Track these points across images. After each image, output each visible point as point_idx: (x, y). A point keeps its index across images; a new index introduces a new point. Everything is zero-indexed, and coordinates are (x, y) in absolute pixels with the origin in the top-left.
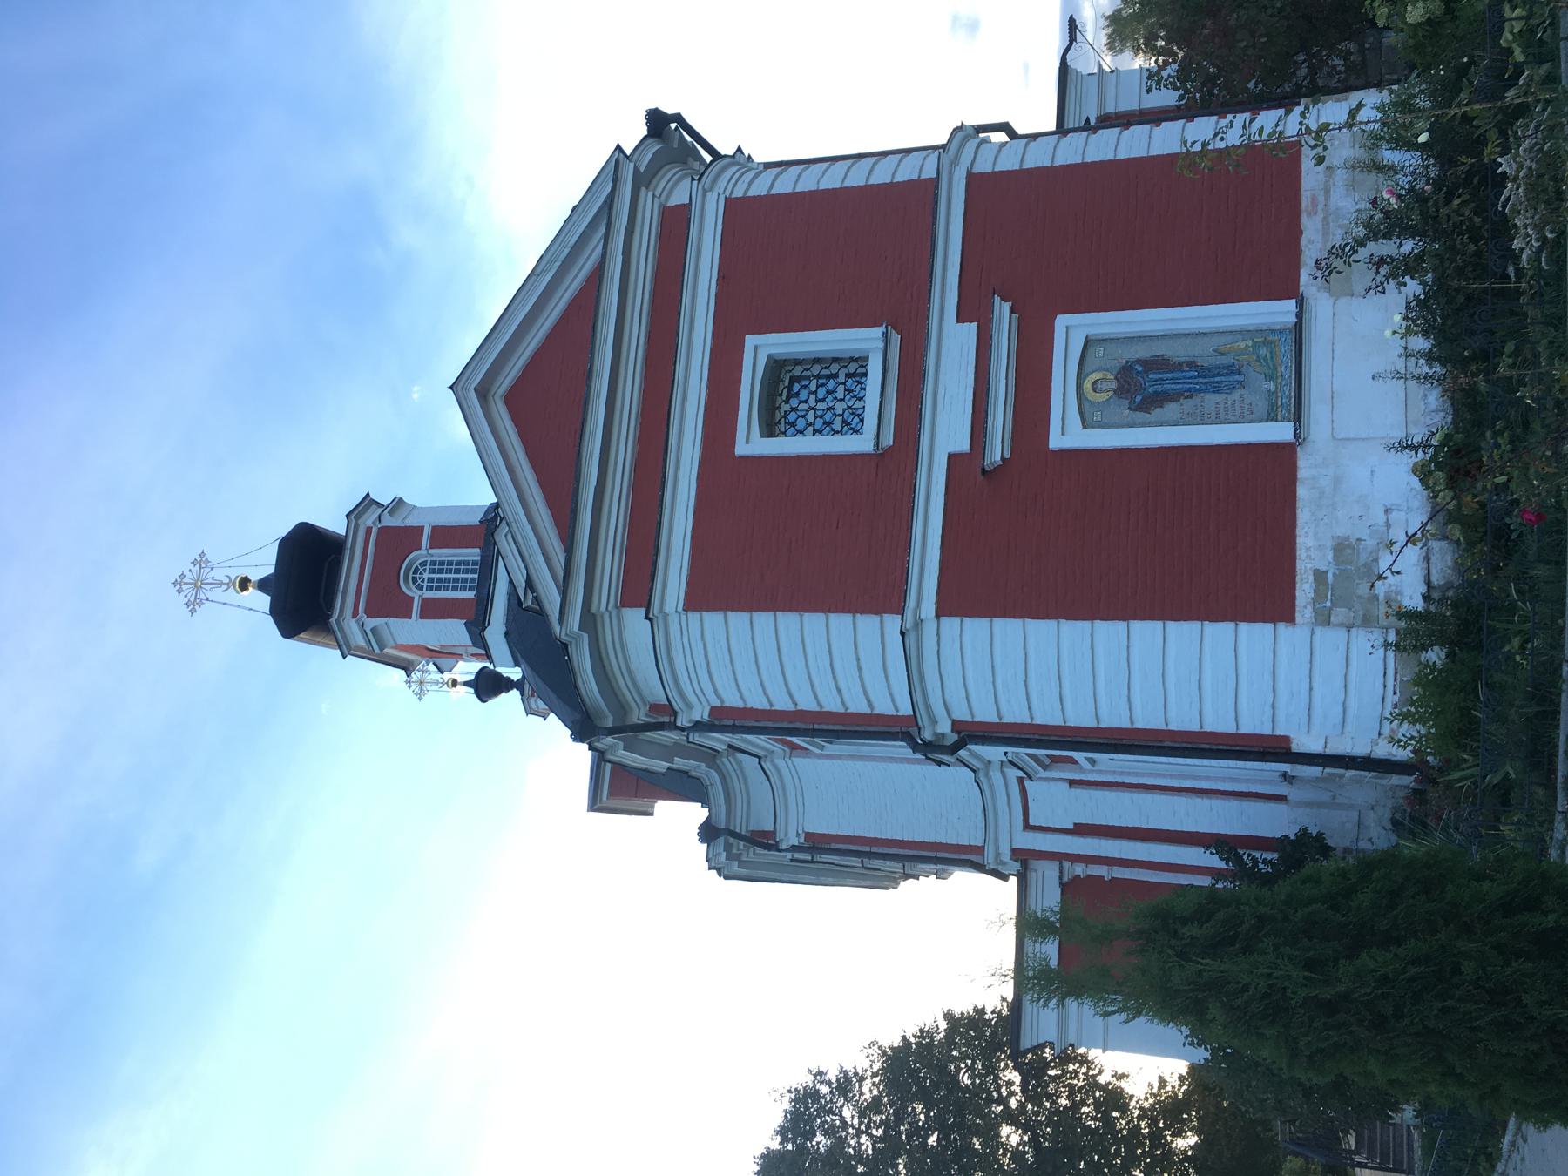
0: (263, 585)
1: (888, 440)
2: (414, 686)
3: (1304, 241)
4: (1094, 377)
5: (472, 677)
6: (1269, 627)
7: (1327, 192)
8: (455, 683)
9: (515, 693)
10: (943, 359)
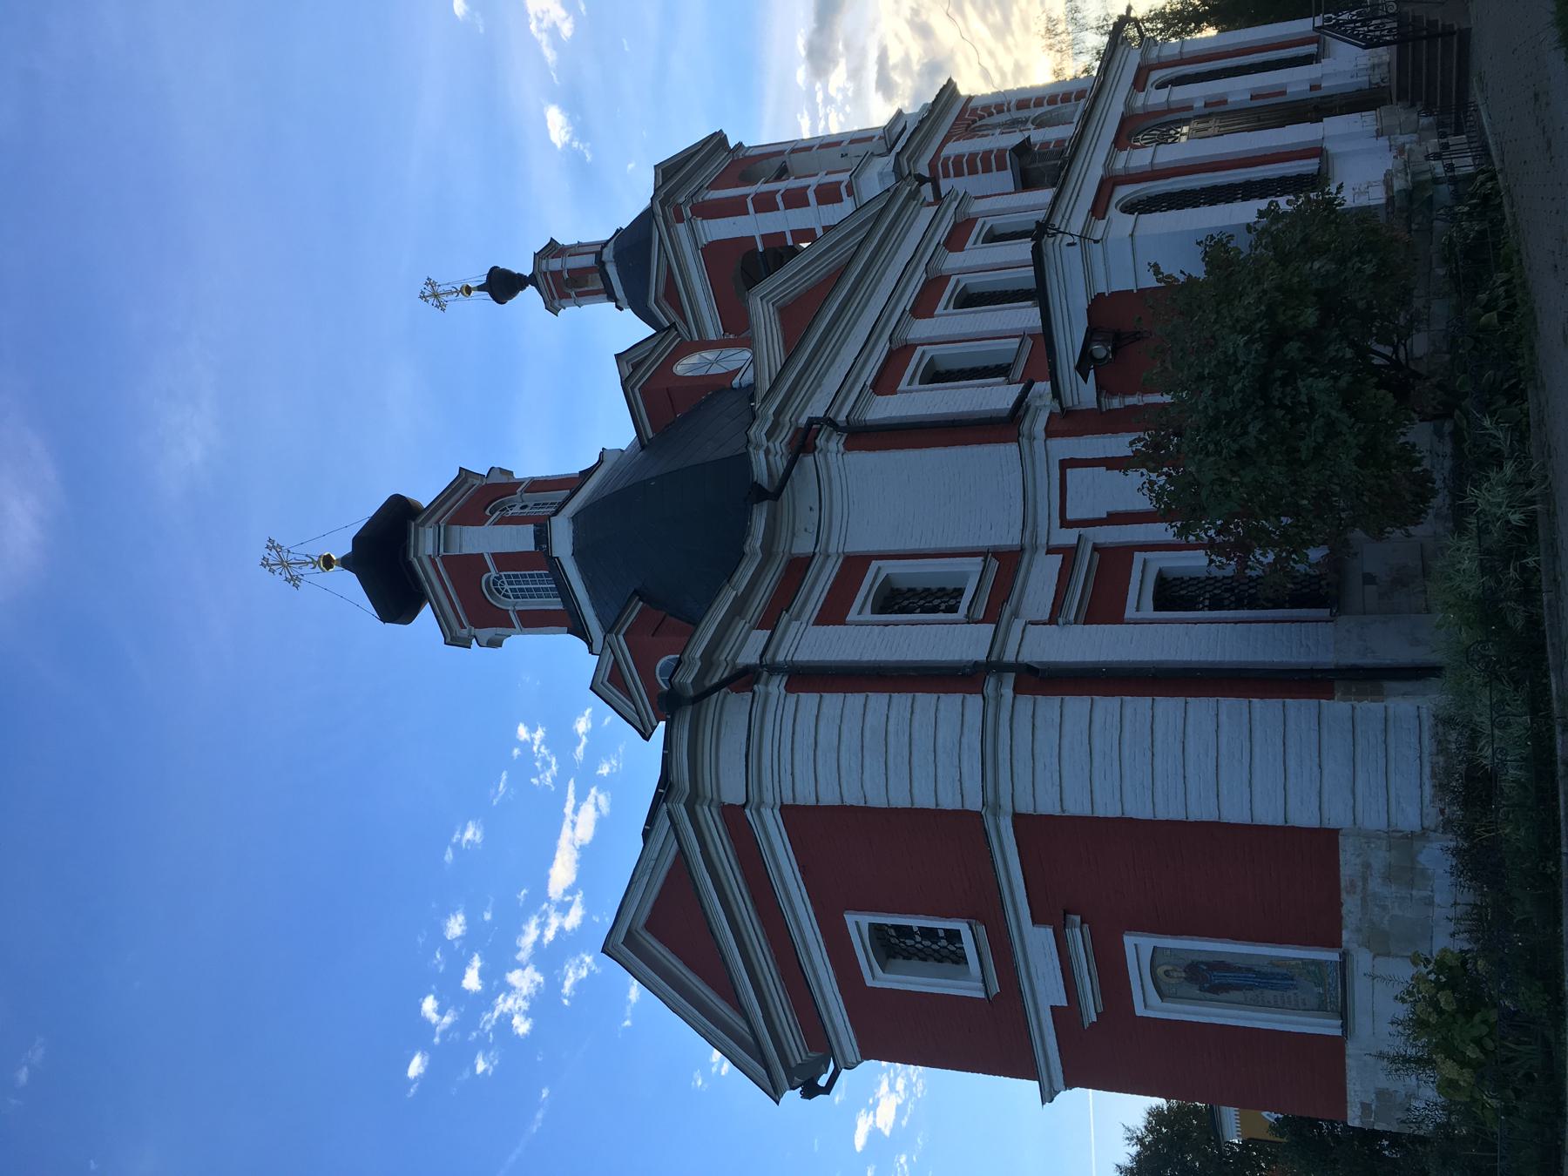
0: (346, 563)
1: (995, 988)
2: (431, 300)
3: (1344, 911)
4: (1165, 968)
5: (484, 279)
6: (1313, 702)
7: (1365, 880)
8: (468, 290)
9: (531, 289)
10: (1029, 950)
